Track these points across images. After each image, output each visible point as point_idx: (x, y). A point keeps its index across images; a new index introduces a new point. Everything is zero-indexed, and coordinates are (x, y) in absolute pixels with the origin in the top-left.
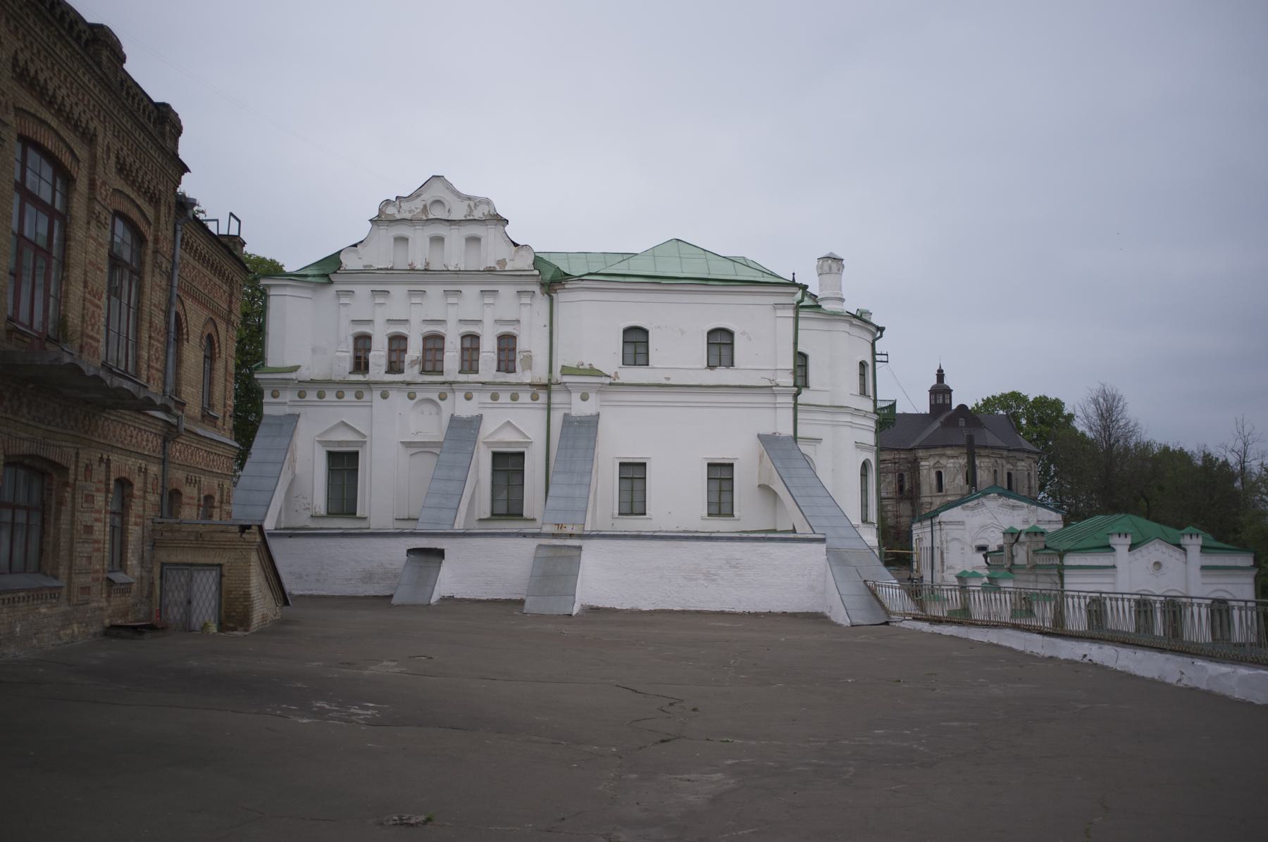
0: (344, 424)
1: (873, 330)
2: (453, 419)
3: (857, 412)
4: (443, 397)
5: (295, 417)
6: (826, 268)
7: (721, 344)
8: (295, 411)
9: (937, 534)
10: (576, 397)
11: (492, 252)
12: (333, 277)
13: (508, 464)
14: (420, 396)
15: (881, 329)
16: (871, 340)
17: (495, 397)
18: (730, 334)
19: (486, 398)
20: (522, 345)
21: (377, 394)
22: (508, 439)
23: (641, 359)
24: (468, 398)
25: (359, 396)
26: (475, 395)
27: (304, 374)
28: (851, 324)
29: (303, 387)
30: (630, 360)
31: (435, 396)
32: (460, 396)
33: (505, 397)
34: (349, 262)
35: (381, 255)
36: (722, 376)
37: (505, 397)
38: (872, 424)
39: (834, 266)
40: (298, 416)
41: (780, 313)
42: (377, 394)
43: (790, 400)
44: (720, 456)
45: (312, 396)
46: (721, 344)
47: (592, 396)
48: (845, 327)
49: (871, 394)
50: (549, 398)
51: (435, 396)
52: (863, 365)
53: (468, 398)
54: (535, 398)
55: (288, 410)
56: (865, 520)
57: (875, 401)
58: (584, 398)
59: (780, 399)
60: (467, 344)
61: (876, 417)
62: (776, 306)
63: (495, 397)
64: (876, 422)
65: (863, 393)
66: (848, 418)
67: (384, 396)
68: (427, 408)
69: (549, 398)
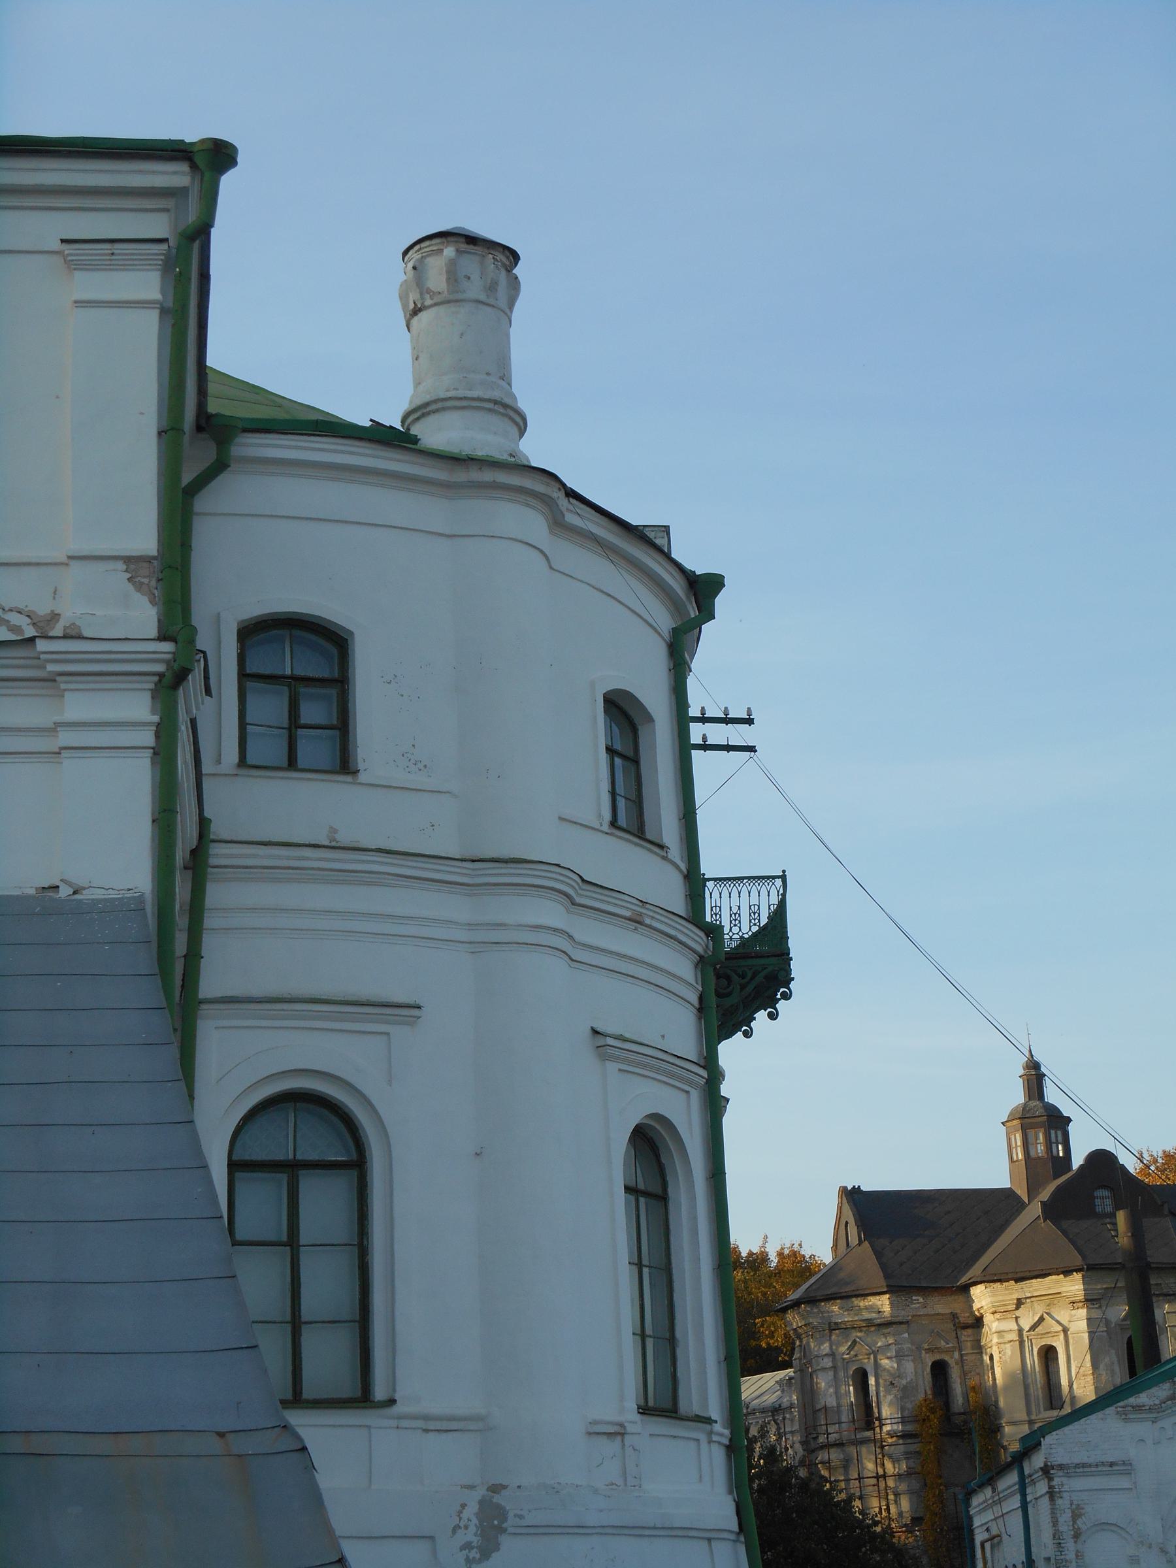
1: (678, 585)
3: (583, 893)
6: (436, 279)
9: (1041, 1512)
15: (703, 590)
16: (666, 622)
28: (558, 524)
38: (685, 968)
39: (471, 264)
41: (92, 285)
43: (137, 707)
48: (529, 522)
49: (670, 831)
52: (622, 711)
56: (662, 1404)
57: (694, 882)
59: (79, 705)
61: (698, 940)
64: (702, 962)
65: (630, 819)
66: (551, 913)
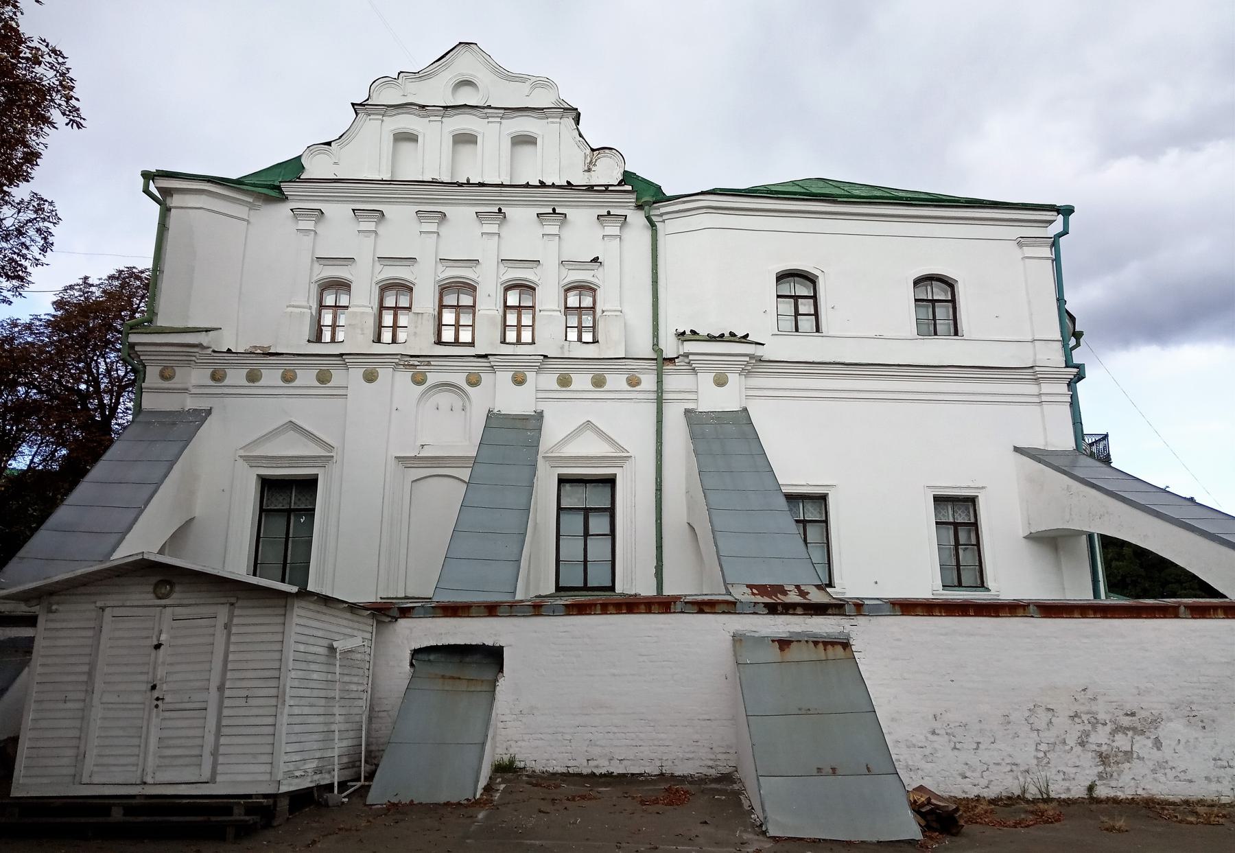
0: (293, 426)
2: (491, 416)
4: (474, 382)
5: (202, 416)
7: (937, 299)
8: (203, 404)
10: (706, 380)
11: (556, 159)
12: (287, 188)
13: (590, 493)
14: (433, 378)
17: (564, 382)
18: (948, 283)
19: (549, 380)
20: (605, 302)
21: (356, 374)
22: (586, 451)
23: (806, 323)
24: (519, 381)
25: (323, 378)
26: (531, 376)
27: (227, 340)
29: (220, 363)
30: (789, 324)
31: (460, 379)
32: (505, 377)
33: (581, 381)
34: (315, 168)
35: (368, 157)
36: (940, 350)
37: (581, 381)
40: (209, 412)
42: (356, 374)
44: (955, 483)
45: (236, 376)
46: (937, 299)
47: (733, 378)
50: (660, 382)
51: (460, 379)
53: (519, 381)
54: (633, 382)
55: (190, 404)
58: (721, 382)
60: (513, 299)
62: (1022, 242)
63: (564, 382)
67: (370, 377)
68: (445, 399)
69: (660, 382)
